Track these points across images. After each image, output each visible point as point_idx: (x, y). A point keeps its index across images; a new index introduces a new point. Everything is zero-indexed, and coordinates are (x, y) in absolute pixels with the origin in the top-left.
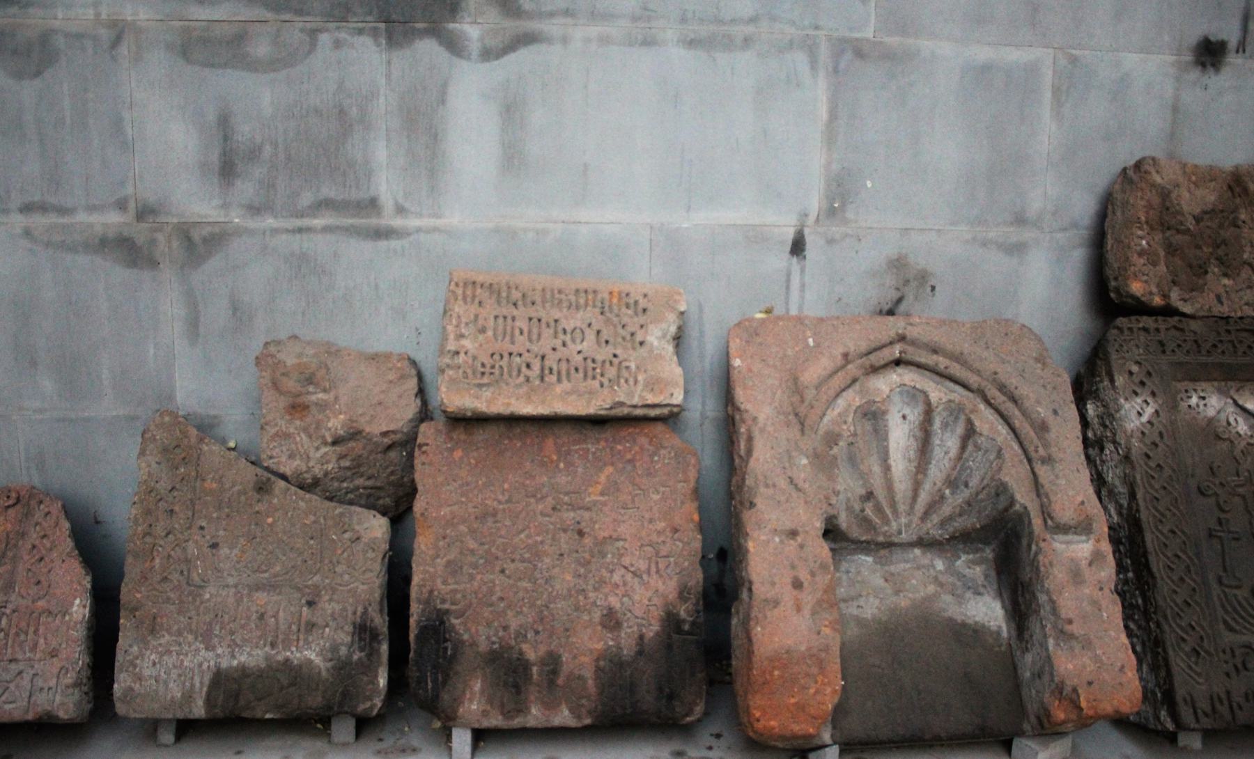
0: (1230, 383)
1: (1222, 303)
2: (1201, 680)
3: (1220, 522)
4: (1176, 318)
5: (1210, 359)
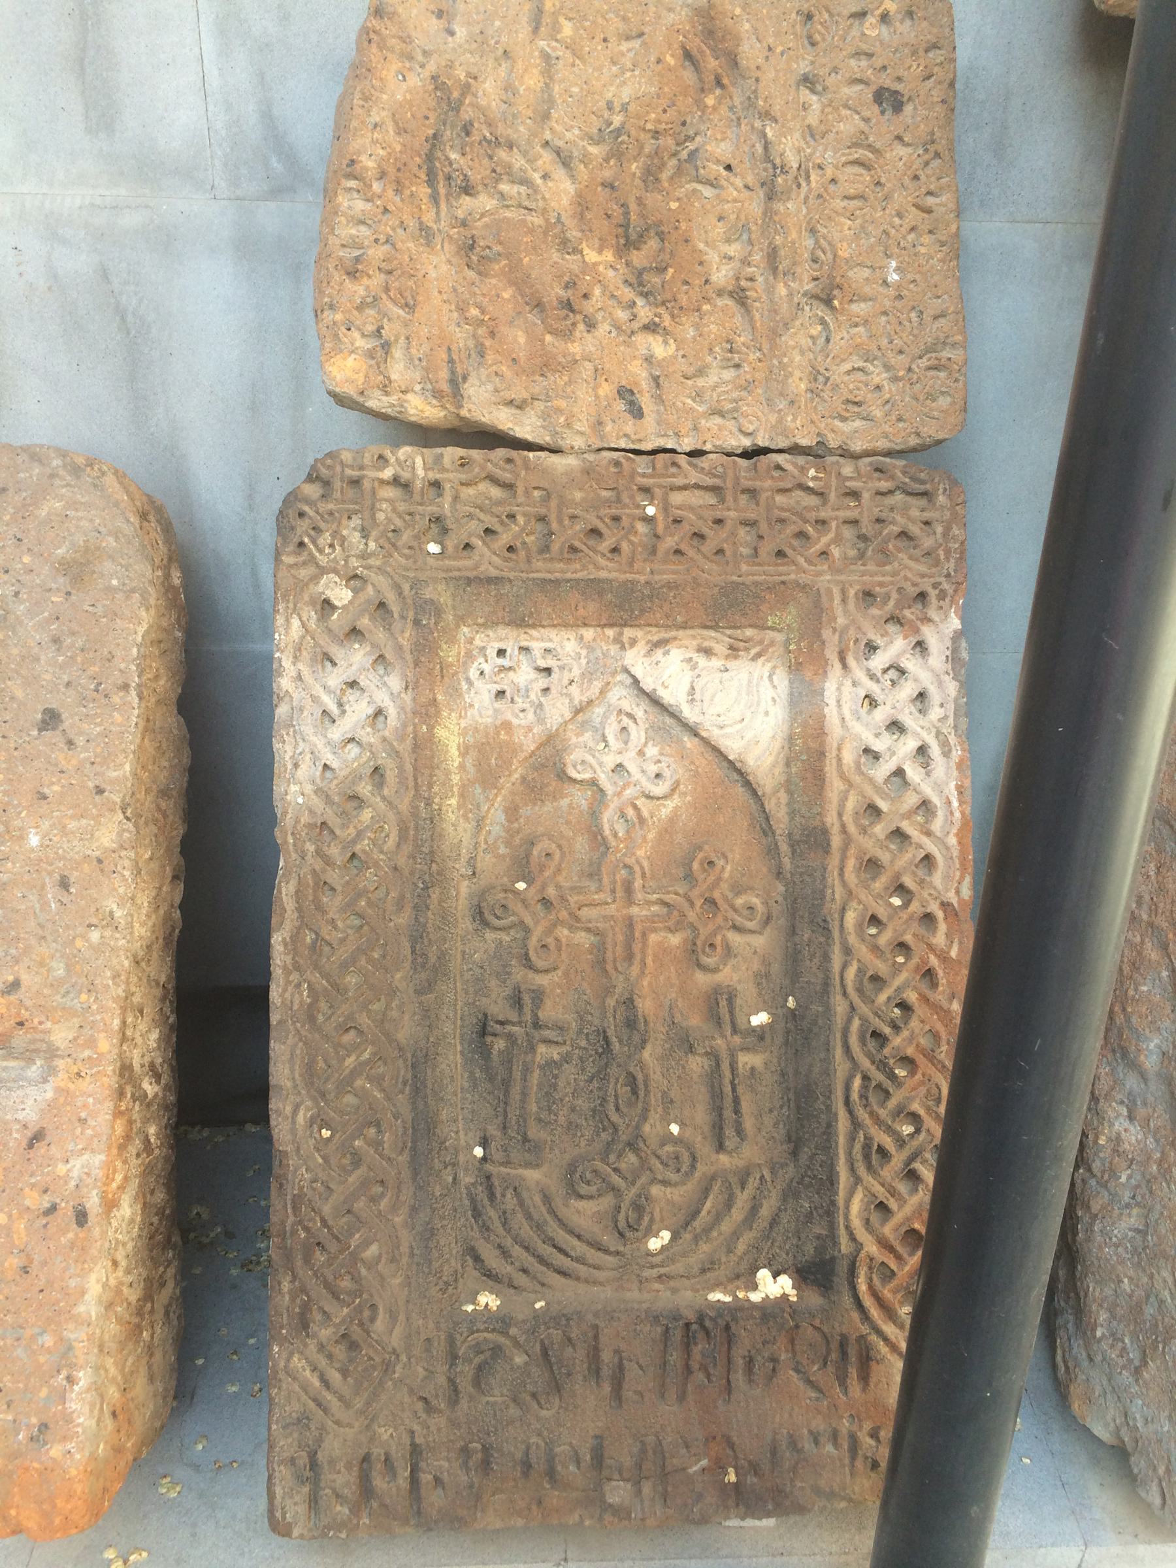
0: (628, 633)
1: (637, 413)
3: (517, 1001)
4: (501, 453)
5: (576, 571)
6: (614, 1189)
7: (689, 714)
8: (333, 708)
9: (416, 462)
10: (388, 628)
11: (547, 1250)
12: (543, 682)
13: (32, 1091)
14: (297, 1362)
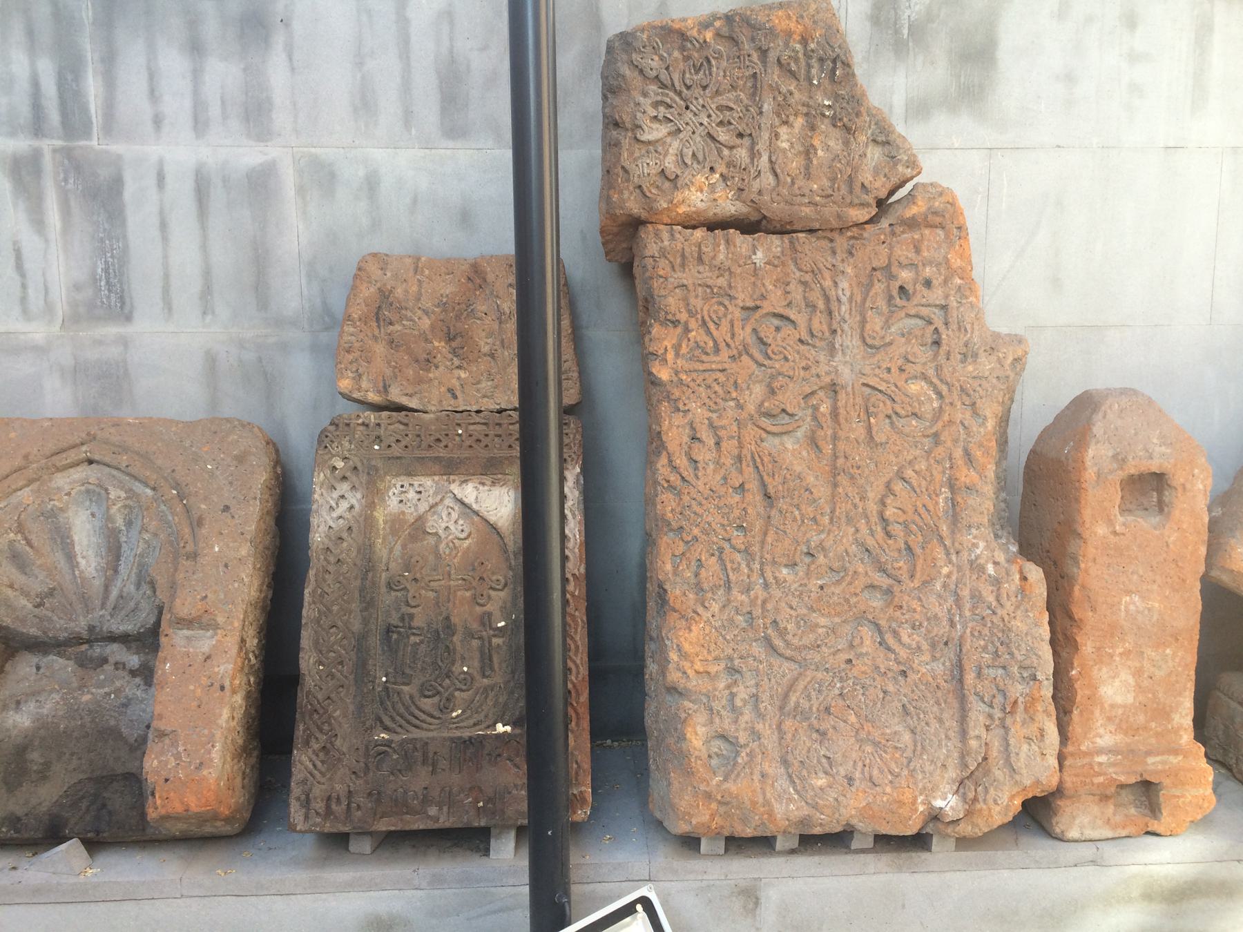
0: (452, 477)
1: (455, 397)
2: (323, 780)
3: (402, 619)
6: (438, 693)
7: (475, 506)
8: (334, 505)
9: (372, 417)
10: (357, 475)
11: (410, 718)
12: (418, 496)
13: (208, 642)
14: (304, 758)
